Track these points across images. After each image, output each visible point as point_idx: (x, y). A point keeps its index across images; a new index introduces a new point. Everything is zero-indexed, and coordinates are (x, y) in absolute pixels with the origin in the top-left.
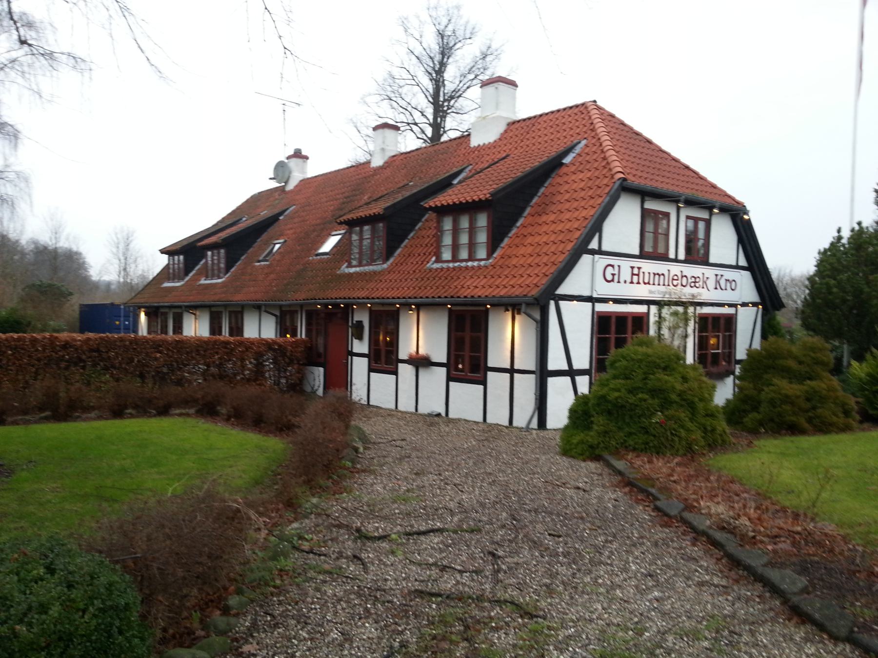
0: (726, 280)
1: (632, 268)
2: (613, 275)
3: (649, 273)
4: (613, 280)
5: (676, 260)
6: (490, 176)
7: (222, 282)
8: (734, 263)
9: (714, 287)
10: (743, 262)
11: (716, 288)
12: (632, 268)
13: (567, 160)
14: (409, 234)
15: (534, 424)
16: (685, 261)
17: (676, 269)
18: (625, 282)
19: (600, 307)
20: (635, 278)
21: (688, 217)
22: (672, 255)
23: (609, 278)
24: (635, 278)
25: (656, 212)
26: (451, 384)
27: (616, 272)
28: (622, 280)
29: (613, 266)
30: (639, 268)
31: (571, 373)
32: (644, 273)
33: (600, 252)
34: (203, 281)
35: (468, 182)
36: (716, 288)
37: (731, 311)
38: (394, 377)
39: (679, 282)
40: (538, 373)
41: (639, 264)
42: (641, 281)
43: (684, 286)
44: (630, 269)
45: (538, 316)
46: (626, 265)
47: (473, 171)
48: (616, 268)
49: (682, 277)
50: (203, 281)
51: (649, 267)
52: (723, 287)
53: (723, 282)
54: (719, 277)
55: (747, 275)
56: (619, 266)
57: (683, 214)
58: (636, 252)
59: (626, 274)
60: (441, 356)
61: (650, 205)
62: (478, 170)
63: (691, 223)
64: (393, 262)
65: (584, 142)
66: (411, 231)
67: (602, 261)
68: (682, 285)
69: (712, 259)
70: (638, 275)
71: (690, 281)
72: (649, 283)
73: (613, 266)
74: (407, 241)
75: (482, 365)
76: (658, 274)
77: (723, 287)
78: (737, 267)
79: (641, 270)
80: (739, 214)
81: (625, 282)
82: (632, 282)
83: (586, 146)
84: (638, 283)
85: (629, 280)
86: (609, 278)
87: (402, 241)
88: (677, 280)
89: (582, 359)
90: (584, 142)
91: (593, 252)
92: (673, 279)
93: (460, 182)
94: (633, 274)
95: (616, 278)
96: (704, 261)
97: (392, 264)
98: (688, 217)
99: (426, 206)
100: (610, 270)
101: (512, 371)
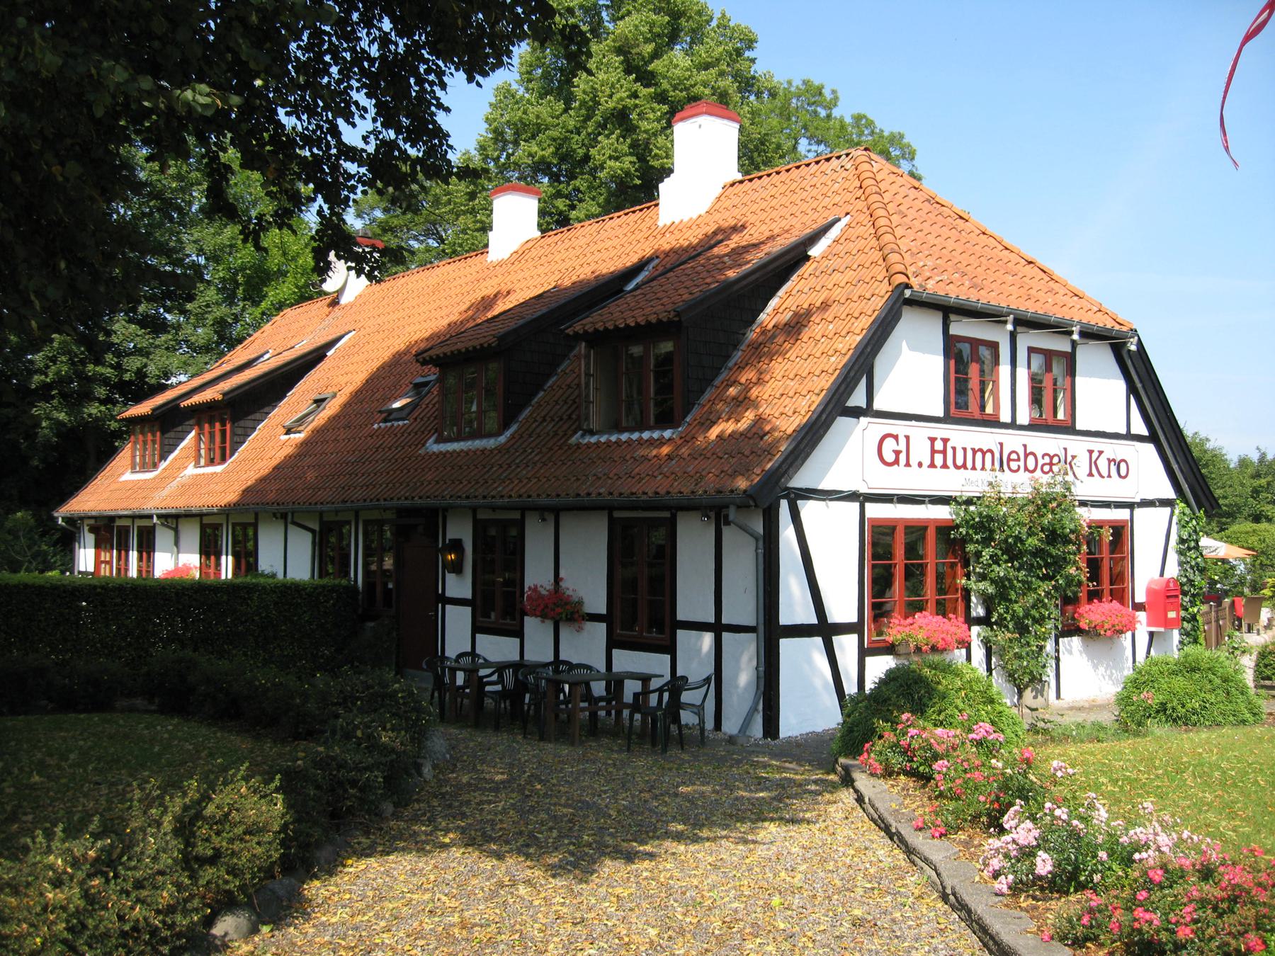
0: (1109, 461)
1: (933, 440)
2: (897, 453)
3: (965, 449)
4: (896, 462)
5: (1013, 425)
6: (684, 278)
7: (500, 449)
8: (1123, 431)
9: (1088, 472)
10: (1139, 428)
11: (1091, 475)
12: (933, 440)
13: (815, 251)
14: (547, 381)
15: (757, 730)
16: (1033, 427)
17: (1013, 441)
18: (920, 465)
19: (876, 511)
20: (939, 459)
21: (1031, 350)
22: (1005, 417)
23: (890, 457)
24: (939, 459)
25: (975, 343)
26: (615, 652)
27: (902, 446)
28: (914, 462)
29: (896, 437)
30: (945, 441)
31: (825, 630)
32: (954, 449)
33: (867, 411)
34: (434, 447)
35: (646, 289)
36: (1091, 475)
37: (1123, 514)
38: (517, 641)
39: (1022, 463)
40: (761, 629)
41: (945, 435)
42: (950, 462)
43: (1032, 472)
44: (929, 442)
45: (759, 527)
46: (920, 434)
47: (661, 269)
48: (902, 441)
49: (1026, 455)
50: (434, 447)
51: (964, 437)
52: (1105, 473)
53: (1103, 464)
54: (1095, 455)
55: (1150, 448)
56: (907, 438)
57: (1024, 342)
58: (940, 413)
59: (921, 451)
60: (597, 601)
61: (962, 328)
62: (668, 266)
63: (1037, 361)
64: (516, 432)
65: (845, 221)
66: (549, 376)
67: (881, 427)
68: (1026, 469)
69: (1079, 427)
70: (944, 452)
71: (1041, 462)
72: (964, 466)
73: (896, 437)
74: (541, 394)
75: (667, 620)
76: (980, 450)
77: (1104, 472)
78: (1129, 436)
79: (949, 445)
80: (1125, 343)
81: (920, 465)
82: (932, 465)
83: (849, 225)
84: (945, 466)
85: (927, 462)
86: (890, 457)
87: (534, 394)
88: (1018, 460)
89: (843, 607)
90: (845, 221)
91: (857, 413)
92: (1009, 460)
93: (637, 287)
94: (933, 452)
95: (903, 457)
96: (1068, 428)
97: (513, 436)
98: (1031, 350)
99: (570, 331)
100: (889, 445)
101: (718, 628)
